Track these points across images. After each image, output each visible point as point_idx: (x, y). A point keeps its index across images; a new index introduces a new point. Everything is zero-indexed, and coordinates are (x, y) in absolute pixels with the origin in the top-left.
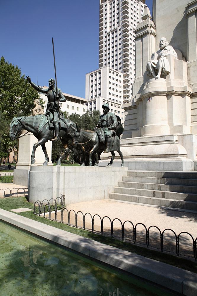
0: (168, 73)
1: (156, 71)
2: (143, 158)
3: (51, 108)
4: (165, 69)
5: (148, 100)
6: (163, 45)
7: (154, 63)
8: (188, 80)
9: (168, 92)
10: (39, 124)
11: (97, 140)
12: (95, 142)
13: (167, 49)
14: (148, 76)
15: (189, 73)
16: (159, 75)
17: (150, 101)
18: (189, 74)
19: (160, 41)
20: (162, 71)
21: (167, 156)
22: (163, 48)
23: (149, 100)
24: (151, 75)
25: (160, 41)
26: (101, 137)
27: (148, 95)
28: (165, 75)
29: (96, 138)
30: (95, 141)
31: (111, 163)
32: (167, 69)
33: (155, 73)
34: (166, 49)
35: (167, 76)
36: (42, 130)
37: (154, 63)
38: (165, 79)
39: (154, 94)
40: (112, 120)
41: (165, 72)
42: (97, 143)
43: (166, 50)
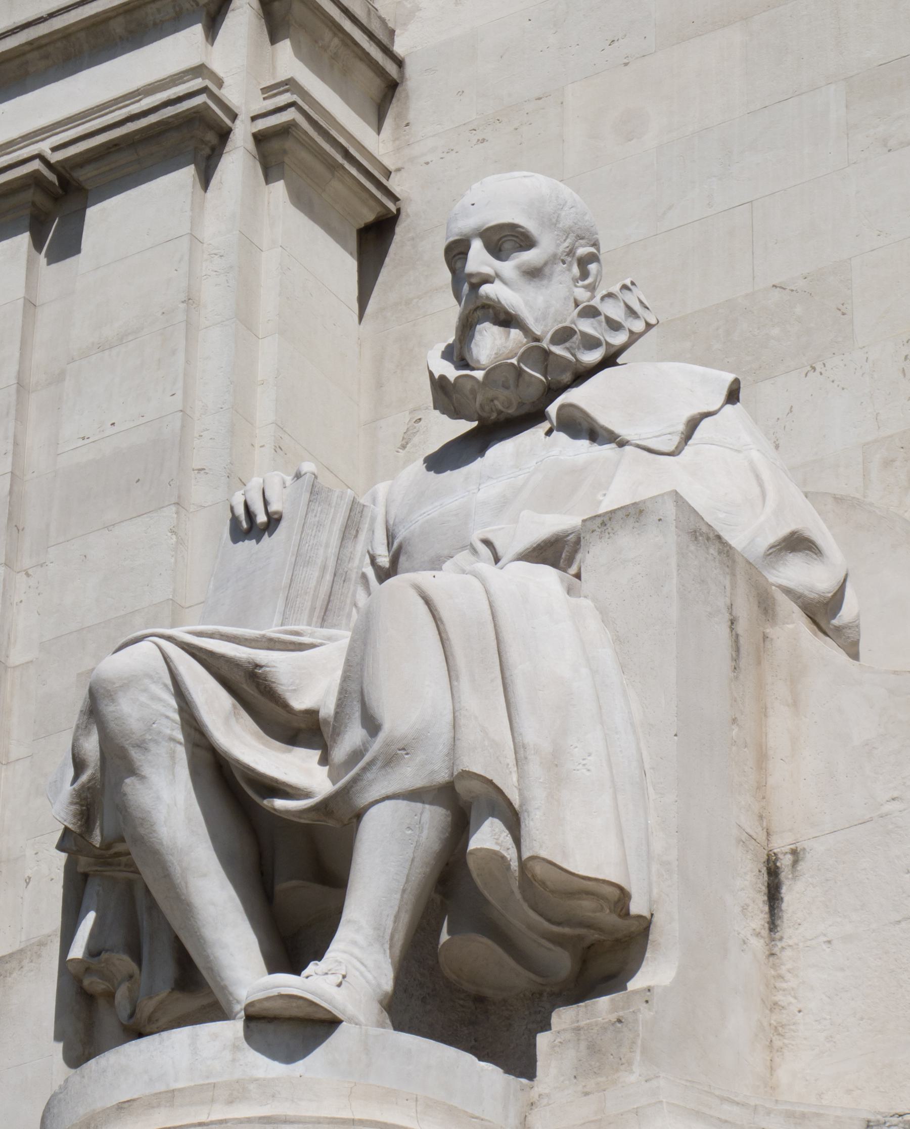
0: (597, 947)
1: (292, 872)
4: (513, 821)
6: (506, 319)
7: (252, 691)
13: (605, 418)
19: (456, 252)
22: (506, 401)
25: (456, 252)
32: (582, 831)
35: (564, 1017)
37: (252, 691)
38: (522, 1064)
41: (520, 917)
43: (593, 433)
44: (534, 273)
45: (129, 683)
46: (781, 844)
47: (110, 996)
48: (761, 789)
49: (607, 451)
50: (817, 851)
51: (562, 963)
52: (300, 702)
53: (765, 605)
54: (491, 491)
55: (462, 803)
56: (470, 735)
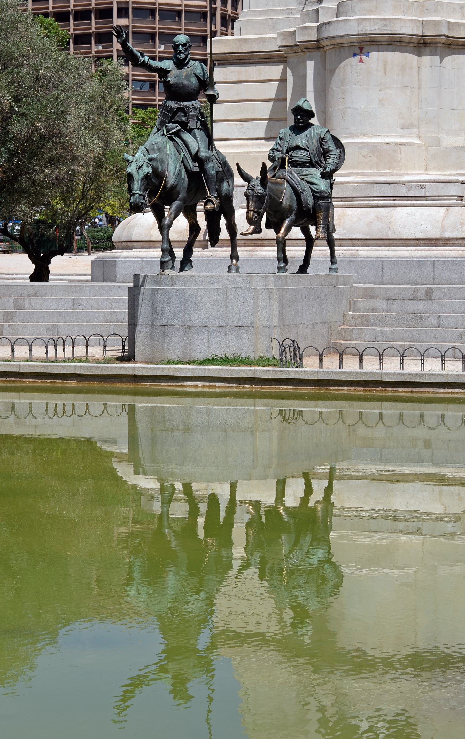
3: (184, 119)
5: (355, 55)
10: (168, 165)
11: (295, 206)
12: (290, 210)
17: (361, 61)
21: (438, 242)
23: (358, 57)
26: (303, 196)
29: (291, 197)
30: (290, 206)
36: (177, 181)
39: (380, 39)
42: (294, 212)
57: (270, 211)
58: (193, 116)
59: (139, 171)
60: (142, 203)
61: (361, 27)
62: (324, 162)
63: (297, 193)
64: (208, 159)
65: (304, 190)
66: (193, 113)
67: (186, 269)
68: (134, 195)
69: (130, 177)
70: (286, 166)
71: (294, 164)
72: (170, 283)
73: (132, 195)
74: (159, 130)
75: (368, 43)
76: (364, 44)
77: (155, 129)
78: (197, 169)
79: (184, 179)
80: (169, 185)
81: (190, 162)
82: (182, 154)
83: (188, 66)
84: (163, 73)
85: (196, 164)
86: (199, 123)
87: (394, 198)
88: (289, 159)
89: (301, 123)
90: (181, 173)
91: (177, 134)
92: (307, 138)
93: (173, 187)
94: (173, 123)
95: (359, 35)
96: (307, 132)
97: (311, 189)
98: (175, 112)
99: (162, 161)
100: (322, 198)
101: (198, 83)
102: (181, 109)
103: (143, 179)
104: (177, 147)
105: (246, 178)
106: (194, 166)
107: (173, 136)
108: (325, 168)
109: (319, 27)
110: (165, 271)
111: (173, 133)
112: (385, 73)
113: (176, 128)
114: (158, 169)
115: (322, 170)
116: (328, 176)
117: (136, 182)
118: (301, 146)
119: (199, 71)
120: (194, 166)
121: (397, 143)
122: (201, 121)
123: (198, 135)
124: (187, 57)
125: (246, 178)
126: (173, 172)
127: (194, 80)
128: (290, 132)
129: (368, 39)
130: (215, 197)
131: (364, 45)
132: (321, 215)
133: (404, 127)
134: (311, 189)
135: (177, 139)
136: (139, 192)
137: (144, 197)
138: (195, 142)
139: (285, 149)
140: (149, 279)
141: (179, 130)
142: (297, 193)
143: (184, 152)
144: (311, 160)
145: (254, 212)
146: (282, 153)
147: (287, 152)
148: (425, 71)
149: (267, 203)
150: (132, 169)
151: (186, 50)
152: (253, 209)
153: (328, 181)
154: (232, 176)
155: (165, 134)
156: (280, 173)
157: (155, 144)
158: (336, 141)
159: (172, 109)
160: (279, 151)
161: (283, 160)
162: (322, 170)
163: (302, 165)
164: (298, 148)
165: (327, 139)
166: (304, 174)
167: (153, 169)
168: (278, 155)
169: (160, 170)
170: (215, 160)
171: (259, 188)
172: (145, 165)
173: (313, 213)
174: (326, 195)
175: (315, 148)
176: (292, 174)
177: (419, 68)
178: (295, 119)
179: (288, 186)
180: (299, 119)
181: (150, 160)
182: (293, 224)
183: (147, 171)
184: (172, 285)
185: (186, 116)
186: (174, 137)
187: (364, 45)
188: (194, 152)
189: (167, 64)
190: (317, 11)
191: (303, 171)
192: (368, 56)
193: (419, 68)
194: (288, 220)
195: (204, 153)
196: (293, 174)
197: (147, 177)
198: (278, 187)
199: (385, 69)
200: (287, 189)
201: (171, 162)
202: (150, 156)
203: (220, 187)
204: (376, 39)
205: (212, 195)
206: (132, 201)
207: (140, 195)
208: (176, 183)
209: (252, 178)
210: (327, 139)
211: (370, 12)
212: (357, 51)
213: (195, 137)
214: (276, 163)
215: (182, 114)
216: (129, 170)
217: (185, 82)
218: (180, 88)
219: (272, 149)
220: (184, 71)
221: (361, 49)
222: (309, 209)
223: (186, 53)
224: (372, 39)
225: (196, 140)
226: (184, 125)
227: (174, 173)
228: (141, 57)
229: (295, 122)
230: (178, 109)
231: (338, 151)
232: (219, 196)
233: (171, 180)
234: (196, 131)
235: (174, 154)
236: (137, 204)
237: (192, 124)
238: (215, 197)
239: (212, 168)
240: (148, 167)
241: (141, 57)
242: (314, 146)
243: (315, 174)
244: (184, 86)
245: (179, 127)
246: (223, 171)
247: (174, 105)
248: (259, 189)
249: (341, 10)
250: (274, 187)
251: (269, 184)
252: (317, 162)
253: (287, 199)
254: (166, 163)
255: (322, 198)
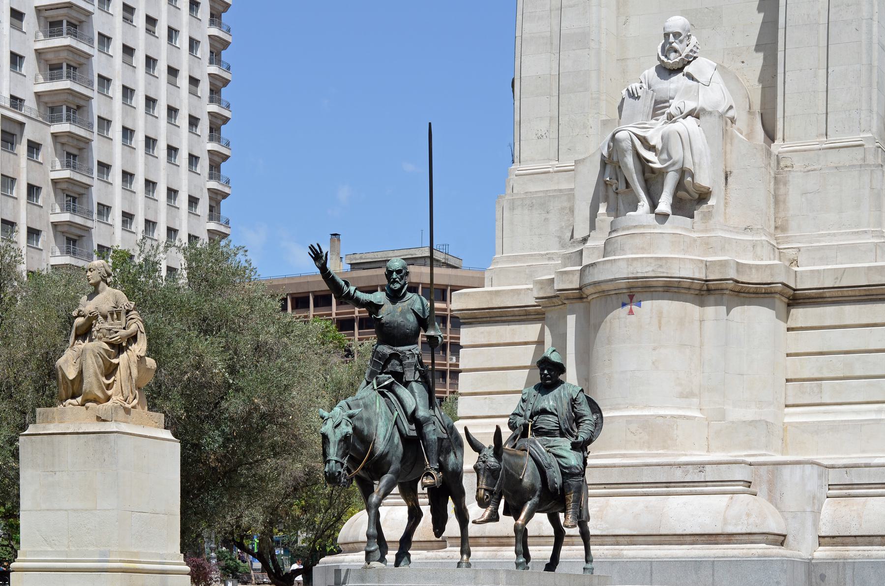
0: (703, 196)
2: (618, 544)
3: (399, 369)
4: (693, 176)
5: (624, 305)
6: (676, 51)
8: (776, 228)
9: (707, 281)
11: (539, 485)
12: (533, 491)
13: (696, 76)
14: (607, 191)
15: (781, 198)
16: (665, 204)
17: (631, 312)
18: (784, 202)
20: (680, 185)
23: (627, 308)
24: (622, 187)
25: (667, 35)
26: (549, 472)
27: (624, 286)
28: (691, 199)
29: (533, 474)
30: (533, 485)
31: (552, 564)
32: (704, 179)
33: (643, 183)
34: (690, 77)
37: (644, 141)
38: (692, 217)
39: (654, 284)
40: (575, 413)
41: (691, 188)
42: (538, 493)
44: (681, 42)
45: (624, 140)
46: (728, 170)
47: (611, 185)
48: (725, 160)
49: (695, 83)
50: (735, 172)
51: (697, 196)
52: (652, 143)
53: (726, 124)
54: (673, 86)
55: (683, 172)
56: (686, 161)
57: (506, 490)
58: (410, 365)
59: (336, 430)
60: (340, 472)
61: (631, 269)
62: (576, 430)
63: (541, 469)
64: (427, 420)
65: (550, 465)
66: (410, 360)
67: (402, 564)
68: (329, 461)
69: (325, 437)
70: (529, 436)
71: (539, 432)
72: (377, 579)
73: (326, 461)
74: (368, 383)
75: (639, 290)
76: (634, 290)
77: (364, 382)
78: (414, 434)
79: (397, 446)
80: (378, 453)
81: (405, 425)
82: (396, 413)
83: (405, 299)
84: (374, 308)
85: (413, 427)
86: (417, 374)
87: (668, 484)
88: (533, 426)
89: (549, 379)
90: (393, 438)
91: (390, 387)
92: (555, 399)
93: (383, 456)
94: (386, 373)
95: (628, 278)
96: (556, 391)
97: (559, 464)
98: (388, 359)
99: (369, 421)
100: (572, 475)
101: (416, 322)
102: (395, 356)
103: (340, 441)
104: (389, 405)
105: (476, 447)
106: (410, 429)
107: (385, 391)
108: (577, 438)
109: (582, 271)
110: (371, 563)
111: (384, 387)
112: (660, 327)
113: (388, 380)
114: (363, 431)
115: (573, 440)
116: (581, 447)
117: (331, 445)
118: (548, 409)
119: (417, 306)
120: (410, 429)
121: (673, 417)
122: (420, 371)
123: (416, 390)
124: (402, 287)
125: (476, 447)
126: (383, 436)
127: (412, 318)
128: (535, 392)
129: (640, 284)
130: (435, 469)
131: (635, 291)
132: (571, 497)
133: (682, 396)
134: (559, 464)
135: (390, 395)
136: (336, 458)
137: (342, 465)
138: (413, 398)
139: (528, 414)
140: (352, 574)
141: (393, 382)
142: (541, 469)
143: (399, 411)
144: (560, 427)
145: (485, 490)
146: (525, 419)
147: (532, 417)
148: (709, 325)
149: (502, 479)
150: (327, 428)
151: (402, 278)
152: (484, 486)
153: (581, 454)
154: (461, 446)
155: (376, 387)
156: (521, 443)
157: (361, 399)
158: (595, 408)
159: (384, 355)
160: (521, 416)
161: (526, 426)
162: (573, 440)
163: (549, 433)
164: (544, 412)
165: (580, 400)
166: (551, 445)
167: (354, 428)
168: (520, 421)
169: (366, 433)
170: (437, 422)
171: (493, 459)
172: (344, 422)
173: (561, 495)
174: (577, 471)
175: (565, 412)
176: (535, 444)
177: (702, 321)
178: (541, 374)
179: (531, 459)
180: (546, 375)
181: (351, 417)
182: (537, 508)
183: (346, 431)
184: (379, 581)
185: (401, 364)
186: (384, 391)
187: (635, 291)
188: (410, 411)
189: (379, 297)
190: (581, 251)
191: (550, 441)
192: (640, 306)
193: (702, 321)
194: (529, 502)
195: (422, 413)
196: (538, 445)
197: (345, 439)
198: (517, 460)
199: (660, 323)
200: (529, 464)
201: (380, 424)
202: (351, 412)
203: (445, 459)
204: (649, 284)
205: (432, 466)
206: (326, 470)
207: (337, 462)
208: (386, 450)
209: (484, 447)
210: (580, 400)
211: (643, 250)
212: (627, 300)
213: (412, 392)
214: (517, 432)
215: (397, 362)
216: (323, 430)
217: (400, 320)
218: (394, 328)
219: (513, 414)
220: (400, 306)
221: (631, 297)
222: (556, 489)
223: (402, 282)
224: (645, 284)
225: (414, 395)
226: (399, 377)
227: (385, 437)
228: (345, 288)
229: (541, 379)
230: (391, 355)
231: (595, 417)
232: (442, 468)
233: (380, 446)
234: (414, 384)
235: (386, 413)
236: (333, 474)
237: (409, 376)
238: (435, 469)
239: (433, 432)
240: (347, 425)
241: (345, 288)
242: (564, 409)
243: (564, 445)
244: (399, 325)
245: (393, 379)
246: (448, 438)
247: (386, 350)
248: (492, 461)
249: (609, 249)
250: (512, 460)
251: (504, 455)
252: (567, 430)
253: (528, 476)
254: (374, 424)
255: (572, 475)
